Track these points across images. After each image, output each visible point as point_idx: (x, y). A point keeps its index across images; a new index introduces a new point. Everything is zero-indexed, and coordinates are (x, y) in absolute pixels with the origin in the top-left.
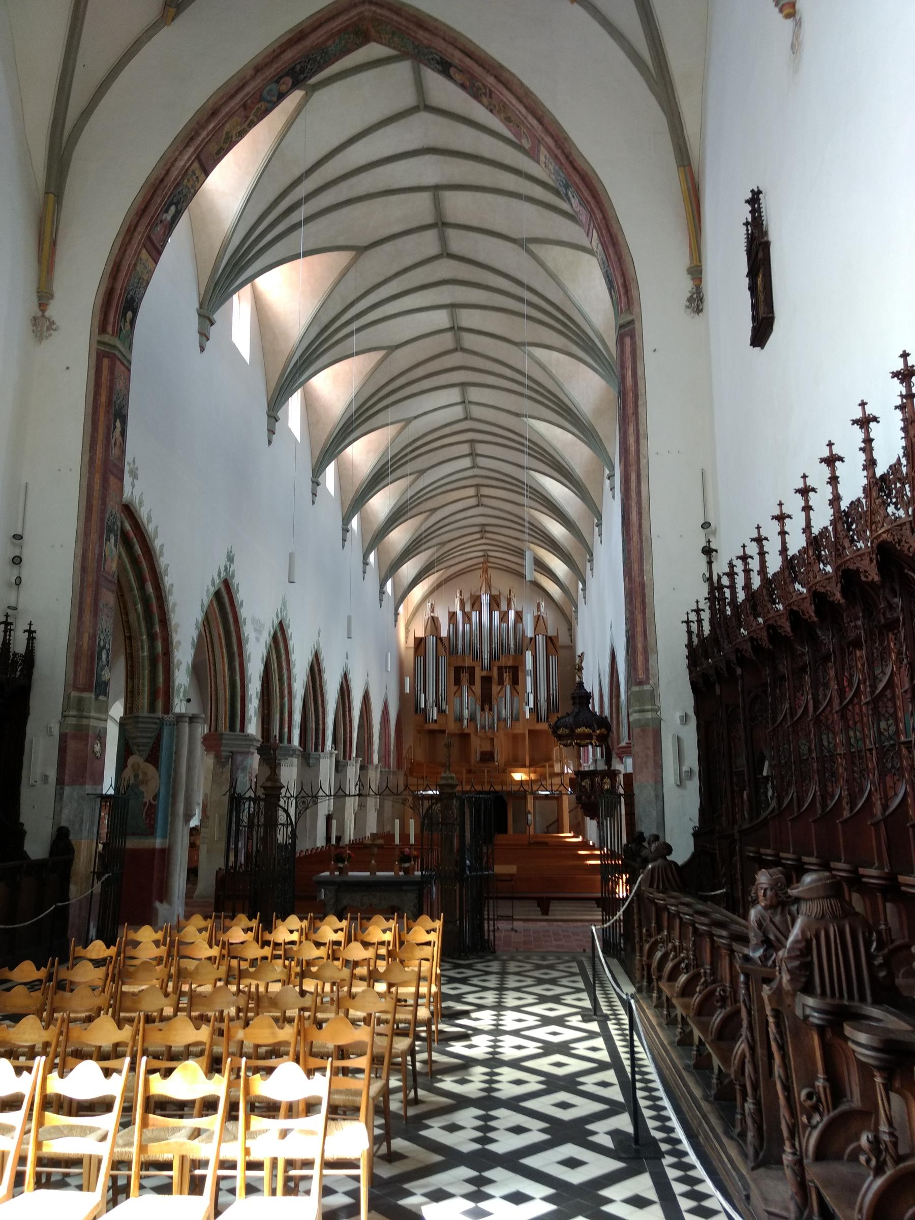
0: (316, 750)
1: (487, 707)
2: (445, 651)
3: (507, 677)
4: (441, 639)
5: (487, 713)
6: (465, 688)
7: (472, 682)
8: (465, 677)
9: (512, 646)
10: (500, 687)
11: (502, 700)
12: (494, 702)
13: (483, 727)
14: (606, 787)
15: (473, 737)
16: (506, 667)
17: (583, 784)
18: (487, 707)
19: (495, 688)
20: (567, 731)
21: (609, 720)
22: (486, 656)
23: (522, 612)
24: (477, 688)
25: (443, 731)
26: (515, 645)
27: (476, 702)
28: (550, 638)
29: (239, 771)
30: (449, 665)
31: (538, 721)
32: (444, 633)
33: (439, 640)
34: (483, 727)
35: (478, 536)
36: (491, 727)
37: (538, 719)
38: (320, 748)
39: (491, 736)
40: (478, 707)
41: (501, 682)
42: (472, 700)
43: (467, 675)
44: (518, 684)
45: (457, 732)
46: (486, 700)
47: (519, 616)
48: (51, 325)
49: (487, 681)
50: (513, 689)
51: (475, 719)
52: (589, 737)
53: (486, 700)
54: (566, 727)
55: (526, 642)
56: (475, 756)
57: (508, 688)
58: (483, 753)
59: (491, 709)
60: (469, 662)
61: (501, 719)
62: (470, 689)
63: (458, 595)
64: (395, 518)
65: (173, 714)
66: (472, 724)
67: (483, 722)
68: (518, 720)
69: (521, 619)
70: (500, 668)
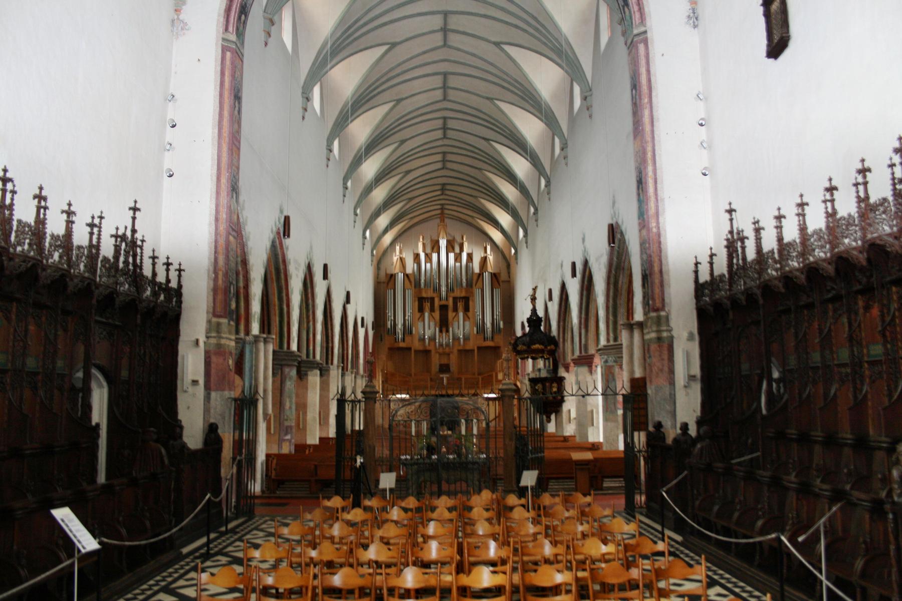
0: (327, 363)
1: (444, 330)
2: (411, 284)
3: (460, 305)
5: (444, 334)
6: (427, 314)
7: (432, 310)
8: (427, 306)
9: (464, 280)
10: (454, 314)
11: (456, 324)
13: (441, 345)
14: (555, 389)
15: (433, 352)
16: (460, 298)
17: (537, 388)
18: (444, 330)
19: (451, 315)
20: (525, 347)
21: (557, 338)
22: (444, 289)
24: (437, 314)
25: (409, 349)
26: (467, 280)
28: (495, 274)
29: (287, 380)
31: (485, 340)
32: (409, 270)
33: (407, 276)
34: (441, 345)
35: (439, 193)
36: (448, 345)
37: (485, 338)
38: (330, 362)
40: (437, 329)
41: (455, 309)
42: (432, 324)
43: (429, 304)
45: (421, 348)
46: (444, 324)
47: (470, 257)
48: (184, 26)
49: (444, 308)
50: (465, 316)
51: (435, 339)
52: (542, 351)
53: (444, 324)
54: (524, 344)
55: (475, 278)
56: (435, 367)
57: (461, 314)
58: (441, 366)
59: (447, 331)
60: (429, 294)
61: (456, 339)
62: (431, 315)
63: (421, 240)
64: (379, 178)
65: (252, 335)
66: (432, 343)
68: (469, 339)
70: (455, 299)
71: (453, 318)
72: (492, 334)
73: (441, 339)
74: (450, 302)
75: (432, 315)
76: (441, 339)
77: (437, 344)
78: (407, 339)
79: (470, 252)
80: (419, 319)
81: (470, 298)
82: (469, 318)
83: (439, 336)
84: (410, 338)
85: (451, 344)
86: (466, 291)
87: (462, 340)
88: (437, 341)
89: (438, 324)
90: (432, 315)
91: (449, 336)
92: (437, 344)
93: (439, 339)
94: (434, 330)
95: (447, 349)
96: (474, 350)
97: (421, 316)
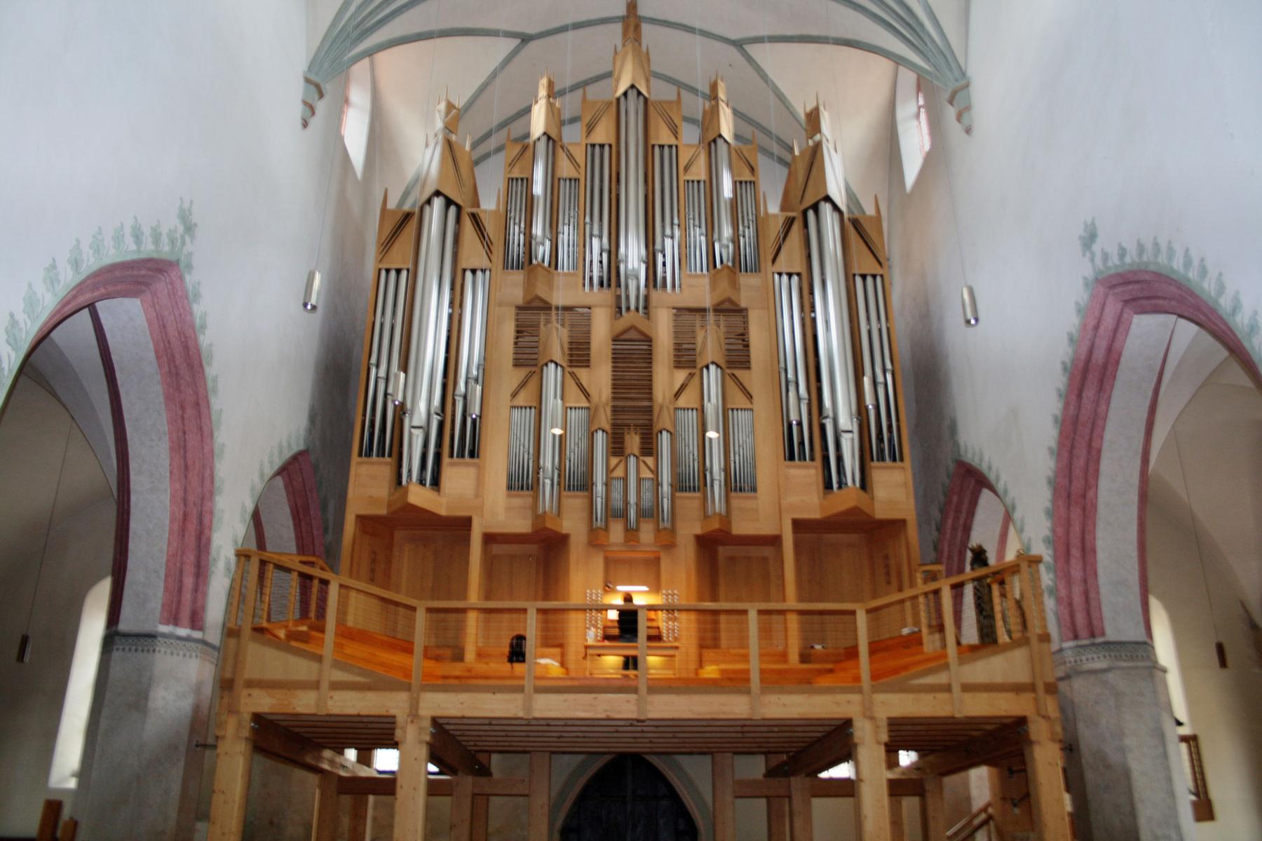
1: (633, 442)
2: (489, 251)
4: (475, 218)
5: (632, 460)
6: (552, 375)
8: (556, 338)
10: (681, 376)
12: (664, 421)
18: (633, 442)
19: (665, 378)
24: (600, 377)
25: (463, 525)
27: (591, 420)
32: (489, 203)
37: (828, 485)
40: (600, 439)
44: (745, 364)
45: (522, 525)
50: (730, 383)
51: (586, 485)
55: (775, 228)
57: (713, 377)
59: (649, 448)
67: (617, 496)
68: (754, 489)
69: (752, 170)
71: (677, 395)
74: (663, 330)
75: (573, 375)
76: (617, 486)
77: (599, 503)
78: (458, 477)
80: (514, 395)
82: (749, 396)
83: (609, 471)
84: (471, 472)
85: (666, 504)
89: (604, 419)
90: (573, 375)
91: (656, 471)
92: (599, 503)
94: (584, 444)
97: (523, 384)
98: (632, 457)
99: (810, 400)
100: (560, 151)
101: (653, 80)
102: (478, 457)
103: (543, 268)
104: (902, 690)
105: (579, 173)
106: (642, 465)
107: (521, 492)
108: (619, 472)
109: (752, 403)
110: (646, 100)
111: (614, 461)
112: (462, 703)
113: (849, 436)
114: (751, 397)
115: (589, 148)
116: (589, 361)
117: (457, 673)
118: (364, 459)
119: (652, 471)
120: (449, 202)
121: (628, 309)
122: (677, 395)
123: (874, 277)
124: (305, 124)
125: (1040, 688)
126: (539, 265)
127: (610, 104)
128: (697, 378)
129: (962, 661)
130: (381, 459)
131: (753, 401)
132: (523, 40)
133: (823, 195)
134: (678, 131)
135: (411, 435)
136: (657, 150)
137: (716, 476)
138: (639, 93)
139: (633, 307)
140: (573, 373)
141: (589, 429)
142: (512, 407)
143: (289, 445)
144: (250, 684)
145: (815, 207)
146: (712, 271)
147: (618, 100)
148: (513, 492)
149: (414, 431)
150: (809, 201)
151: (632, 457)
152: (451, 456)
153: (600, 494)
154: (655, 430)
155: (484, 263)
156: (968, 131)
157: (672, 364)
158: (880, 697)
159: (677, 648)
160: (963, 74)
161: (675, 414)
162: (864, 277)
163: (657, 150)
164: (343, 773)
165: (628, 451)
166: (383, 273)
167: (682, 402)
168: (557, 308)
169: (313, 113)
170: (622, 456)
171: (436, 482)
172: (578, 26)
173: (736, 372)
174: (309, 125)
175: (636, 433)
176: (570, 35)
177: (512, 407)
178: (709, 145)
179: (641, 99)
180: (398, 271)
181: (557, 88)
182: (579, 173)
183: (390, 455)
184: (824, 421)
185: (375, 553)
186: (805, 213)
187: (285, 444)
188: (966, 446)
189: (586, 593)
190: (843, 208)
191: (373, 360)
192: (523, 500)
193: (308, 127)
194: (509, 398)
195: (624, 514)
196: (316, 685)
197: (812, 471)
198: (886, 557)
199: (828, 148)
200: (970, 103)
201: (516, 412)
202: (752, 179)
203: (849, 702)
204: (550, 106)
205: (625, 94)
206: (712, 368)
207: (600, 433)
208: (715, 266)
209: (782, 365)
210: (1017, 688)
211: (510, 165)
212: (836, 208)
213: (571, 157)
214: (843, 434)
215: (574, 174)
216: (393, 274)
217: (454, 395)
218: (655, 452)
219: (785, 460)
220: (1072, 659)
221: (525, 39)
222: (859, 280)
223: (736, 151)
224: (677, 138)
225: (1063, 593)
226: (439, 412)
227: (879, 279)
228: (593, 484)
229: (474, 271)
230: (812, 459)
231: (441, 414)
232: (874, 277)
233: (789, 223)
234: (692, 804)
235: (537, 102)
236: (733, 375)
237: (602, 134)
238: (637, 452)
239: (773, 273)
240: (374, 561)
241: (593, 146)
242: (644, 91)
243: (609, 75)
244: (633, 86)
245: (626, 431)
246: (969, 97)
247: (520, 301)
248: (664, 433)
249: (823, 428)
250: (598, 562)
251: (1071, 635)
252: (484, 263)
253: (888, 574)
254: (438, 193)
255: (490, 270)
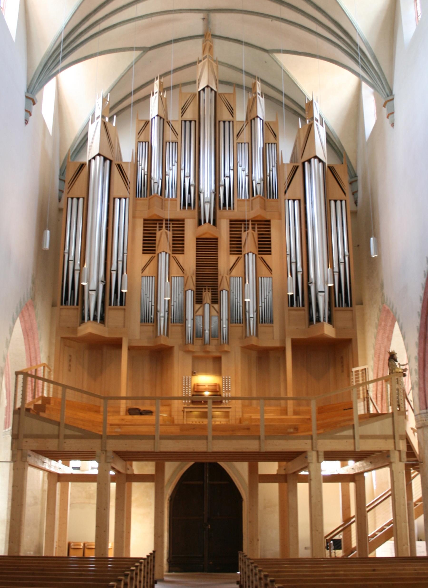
1: (207, 296)
4: (119, 167)
5: (207, 306)
6: (163, 258)
10: (233, 258)
11: (236, 282)
12: (223, 285)
18: (207, 296)
23: (276, 123)
26: (264, 180)
27: (185, 284)
28: (331, 168)
30: (134, 217)
39: (217, 354)
40: (190, 295)
42: (177, 281)
43: (170, 234)
44: (269, 252)
51: (183, 320)
57: (251, 259)
59: (216, 300)
68: (272, 322)
69: (275, 136)
71: (231, 269)
72: (330, 309)
73: (199, 320)
75: (175, 259)
76: (199, 320)
77: (189, 330)
79: (271, 119)
80: (143, 269)
81: (274, 225)
82: (270, 270)
84: (121, 313)
85: (225, 330)
86: (264, 207)
87: (252, 323)
88: (189, 324)
89: (192, 283)
90: (175, 259)
91: (219, 312)
92: (189, 330)
93: (193, 320)
94: (181, 296)
95: (214, 342)
96: (283, 350)
98: (207, 304)
99: (303, 272)
100: (167, 125)
101: (220, 67)
102: (125, 305)
103: (158, 197)
104: (332, 438)
105: (178, 139)
106: (212, 308)
107: (148, 324)
108: (200, 312)
109: (271, 274)
110: (215, 92)
111: (198, 306)
112: (126, 445)
113: (323, 294)
114: (271, 270)
115: (183, 122)
116: (183, 251)
117: (117, 422)
118: (64, 306)
119: (217, 312)
120: (105, 159)
121: (205, 222)
122: (231, 269)
123: (341, 201)
124: (26, 122)
125: (397, 437)
126: (155, 196)
127: (195, 95)
128: (242, 259)
129: (360, 425)
130: (72, 307)
131: (272, 273)
132: (144, 51)
133: (313, 155)
134: (234, 112)
135: (89, 294)
136: (222, 123)
137: (251, 316)
138: (212, 90)
139: (207, 221)
140: (175, 257)
141: (184, 289)
142: (142, 276)
143: (24, 299)
144: (26, 436)
145: (309, 161)
146: (251, 198)
147: (199, 92)
148: (144, 324)
149: (90, 292)
150: (306, 157)
151: (207, 304)
152: (110, 305)
153: (189, 326)
154: (219, 290)
155: (127, 194)
156: (393, 125)
157: (229, 252)
158: (320, 441)
159: (230, 408)
160: (391, 92)
161: (230, 280)
162: (335, 201)
163: (222, 123)
164: (60, 472)
165: (204, 302)
166: (70, 200)
167: (234, 273)
168: (167, 220)
169: (31, 115)
170: (202, 304)
171: (103, 320)
172: (176, 41)
173: (263, 256)
174: (29, 122)
175: (209, 291)
176: (173, 46)
177: (142, 276)
178: (251, 121)
179: (213, 92)
180: (78, 199)
181: (165, 86)
182: (178, 139)
183: (77, 304)
184: (310, 285)
185: (70, 356)
186: (303, 164)
187: (22, 300)
188: (387, 299)
189: (183, 378)
190: (325, 160)
191: (66, 251)
192: (149, 328)
193: (28, 124)
194: (141, 271)
195: (202, 336)
196: (58, 437)
197: (303, 312)
198: (342, 358)
199: (317, 125)
200: (394, 111)
201: (144, 279)
202: (275, 142)
203: (306, 443)
204: (161, 97)
205: (203, 90)
206: (250, 254)
207: (190, 291)
208: (253, 196)
209: (288, 253)
210: (385, 437)
211: (139, 134)
212: (320, 161)
213: (173, 130)
214: (320, 294)
215: (175, 139)
216: (75, 200)
217: (111, 270)
218: (219, 303)
219: (289, 306)
220: (424, 419)
221: (145, 50)
222: (333, 203)
223: (265, 123)
224: (233, 116)
225: (422, 386)
226: (103, 280)
227: (344, 202)
228: (186, 320)
229: (120, 199)
230: (303, 306)
231: (104, 281)
232: (341, 201)
233: (296, 169)
234: (239, 484)
235: (153, 95)
236: (262, 258)
237: (189, 115)
238: (209, 301)
239: (285, 199)
240: (70, 361)
241: (185, 121)
242: (214, 88)
243: (195, 82)
244: (208, 86)
245: (204, 290)
246: (393, 104)
247: (146, 217)
248: (224, 291)
249: (309, 288)
250: (189, 360)
251: (424, 407)
252: (127, 194)
253: (342, 366)
254: (99, 155)
255: (129, 198)
